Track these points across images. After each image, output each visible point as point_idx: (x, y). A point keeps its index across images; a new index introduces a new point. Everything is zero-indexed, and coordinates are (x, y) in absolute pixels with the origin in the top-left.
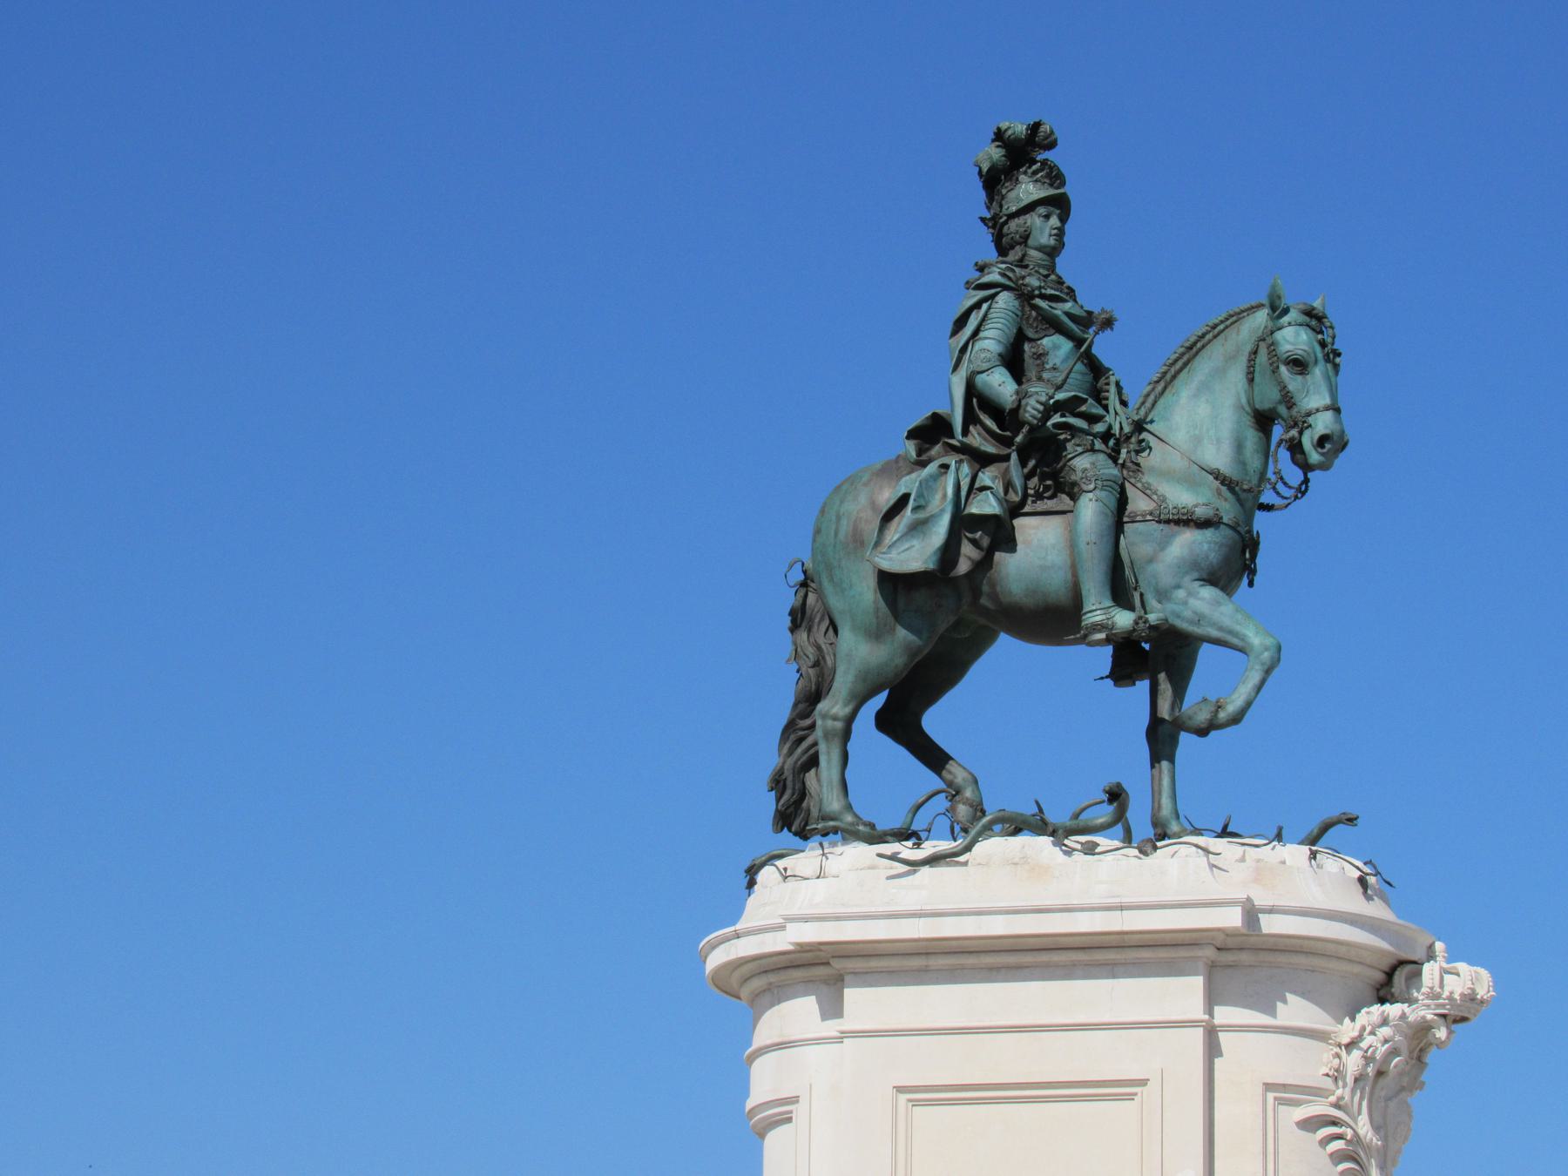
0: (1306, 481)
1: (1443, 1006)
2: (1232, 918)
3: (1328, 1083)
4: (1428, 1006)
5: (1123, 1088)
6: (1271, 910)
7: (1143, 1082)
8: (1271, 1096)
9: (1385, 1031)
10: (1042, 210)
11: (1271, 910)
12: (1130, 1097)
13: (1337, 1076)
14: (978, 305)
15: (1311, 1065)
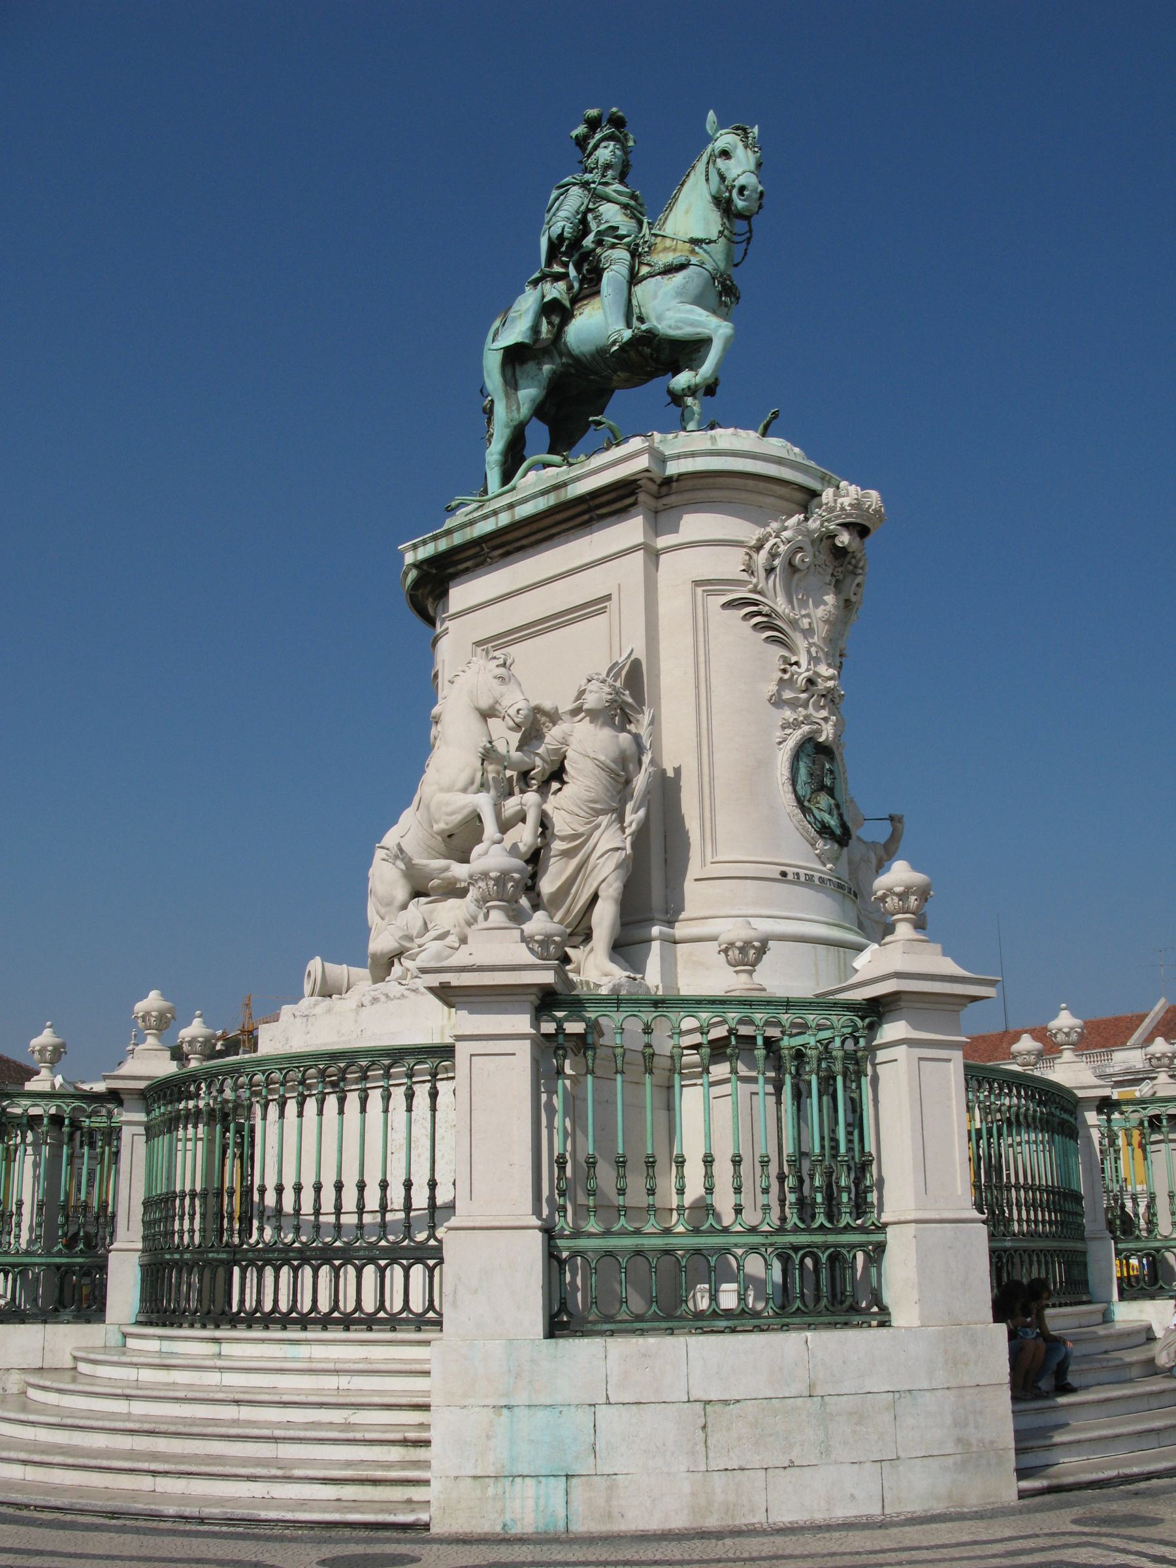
0: (750, 231)
1: (838, 517)
2: (643, 462)
3: (745, 576)
4: (828, 520)
5: (597, 606)
6: (678, 457)
7: (608, 598)
8: (699, 590)
9: (786, 534)
10: (604, 144)
11: (678, 457)
12: (603, 611)
13: (749, 570)
14: (557, 199)
15: (730, 564)
